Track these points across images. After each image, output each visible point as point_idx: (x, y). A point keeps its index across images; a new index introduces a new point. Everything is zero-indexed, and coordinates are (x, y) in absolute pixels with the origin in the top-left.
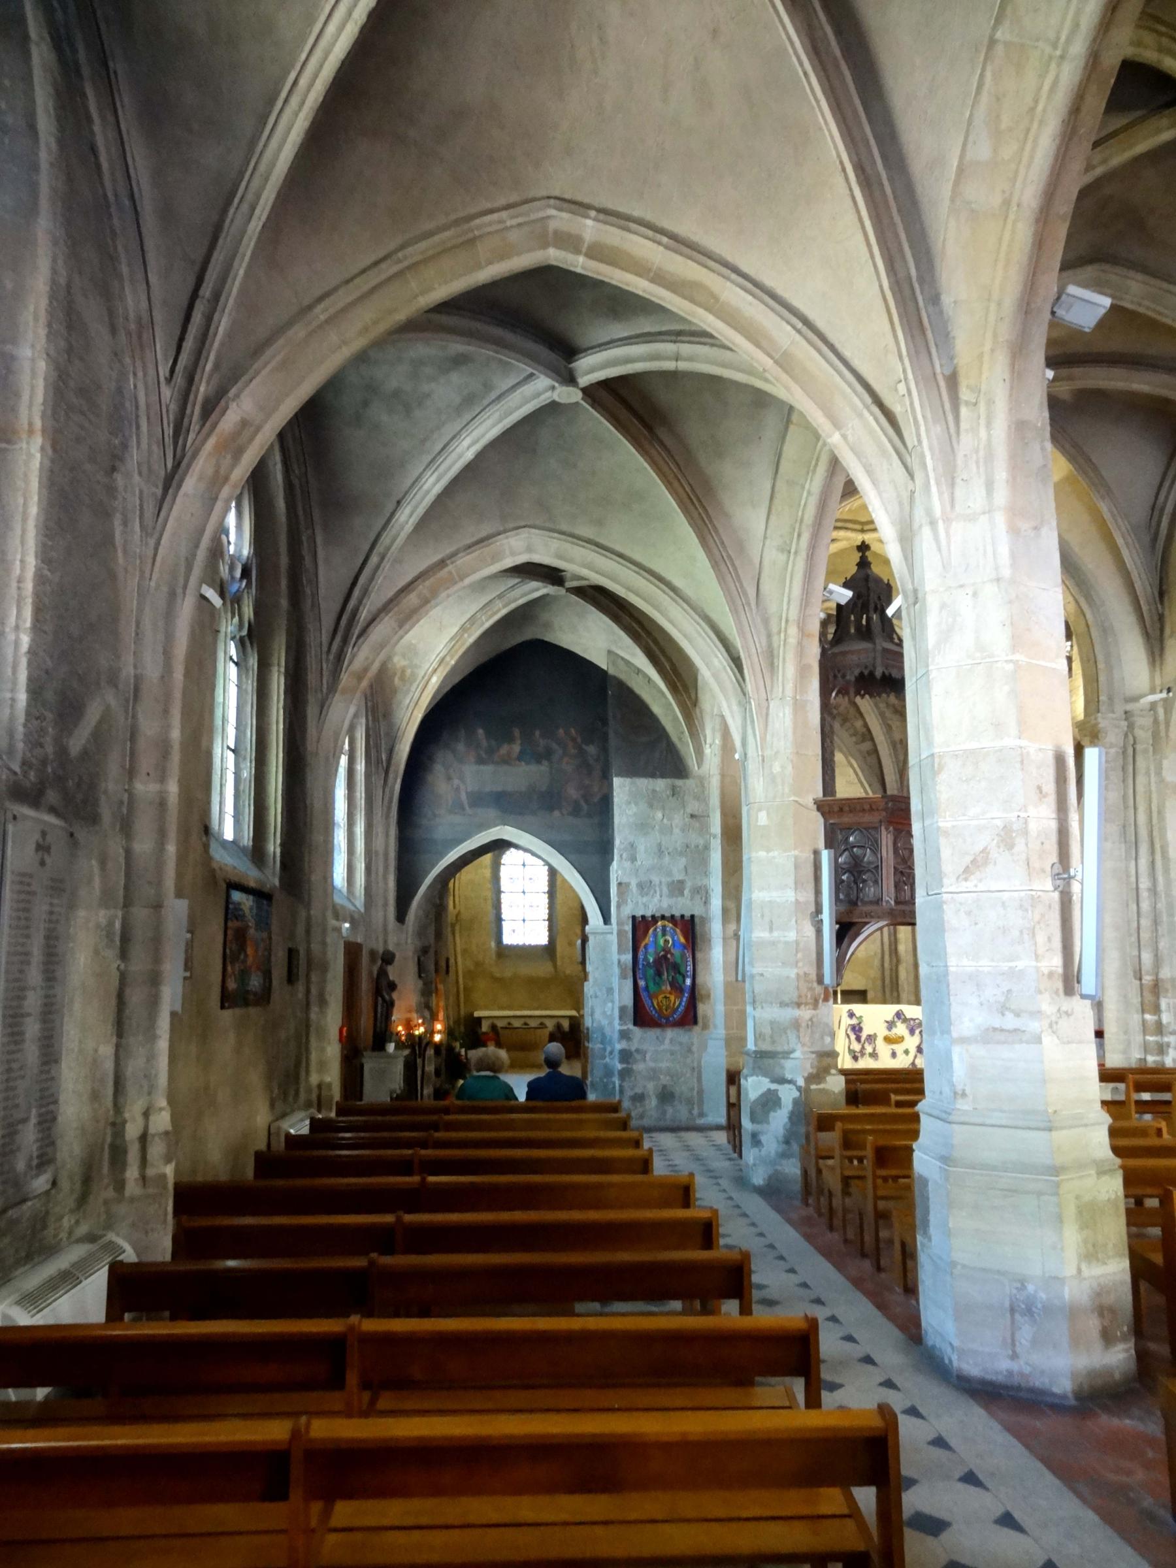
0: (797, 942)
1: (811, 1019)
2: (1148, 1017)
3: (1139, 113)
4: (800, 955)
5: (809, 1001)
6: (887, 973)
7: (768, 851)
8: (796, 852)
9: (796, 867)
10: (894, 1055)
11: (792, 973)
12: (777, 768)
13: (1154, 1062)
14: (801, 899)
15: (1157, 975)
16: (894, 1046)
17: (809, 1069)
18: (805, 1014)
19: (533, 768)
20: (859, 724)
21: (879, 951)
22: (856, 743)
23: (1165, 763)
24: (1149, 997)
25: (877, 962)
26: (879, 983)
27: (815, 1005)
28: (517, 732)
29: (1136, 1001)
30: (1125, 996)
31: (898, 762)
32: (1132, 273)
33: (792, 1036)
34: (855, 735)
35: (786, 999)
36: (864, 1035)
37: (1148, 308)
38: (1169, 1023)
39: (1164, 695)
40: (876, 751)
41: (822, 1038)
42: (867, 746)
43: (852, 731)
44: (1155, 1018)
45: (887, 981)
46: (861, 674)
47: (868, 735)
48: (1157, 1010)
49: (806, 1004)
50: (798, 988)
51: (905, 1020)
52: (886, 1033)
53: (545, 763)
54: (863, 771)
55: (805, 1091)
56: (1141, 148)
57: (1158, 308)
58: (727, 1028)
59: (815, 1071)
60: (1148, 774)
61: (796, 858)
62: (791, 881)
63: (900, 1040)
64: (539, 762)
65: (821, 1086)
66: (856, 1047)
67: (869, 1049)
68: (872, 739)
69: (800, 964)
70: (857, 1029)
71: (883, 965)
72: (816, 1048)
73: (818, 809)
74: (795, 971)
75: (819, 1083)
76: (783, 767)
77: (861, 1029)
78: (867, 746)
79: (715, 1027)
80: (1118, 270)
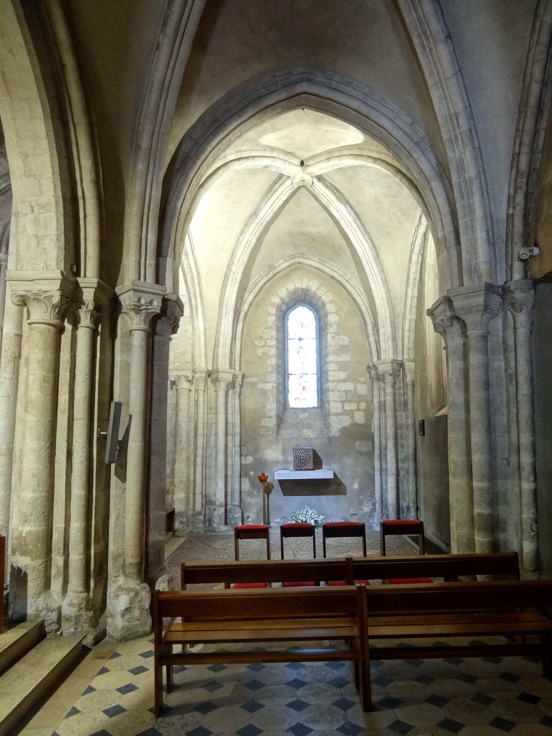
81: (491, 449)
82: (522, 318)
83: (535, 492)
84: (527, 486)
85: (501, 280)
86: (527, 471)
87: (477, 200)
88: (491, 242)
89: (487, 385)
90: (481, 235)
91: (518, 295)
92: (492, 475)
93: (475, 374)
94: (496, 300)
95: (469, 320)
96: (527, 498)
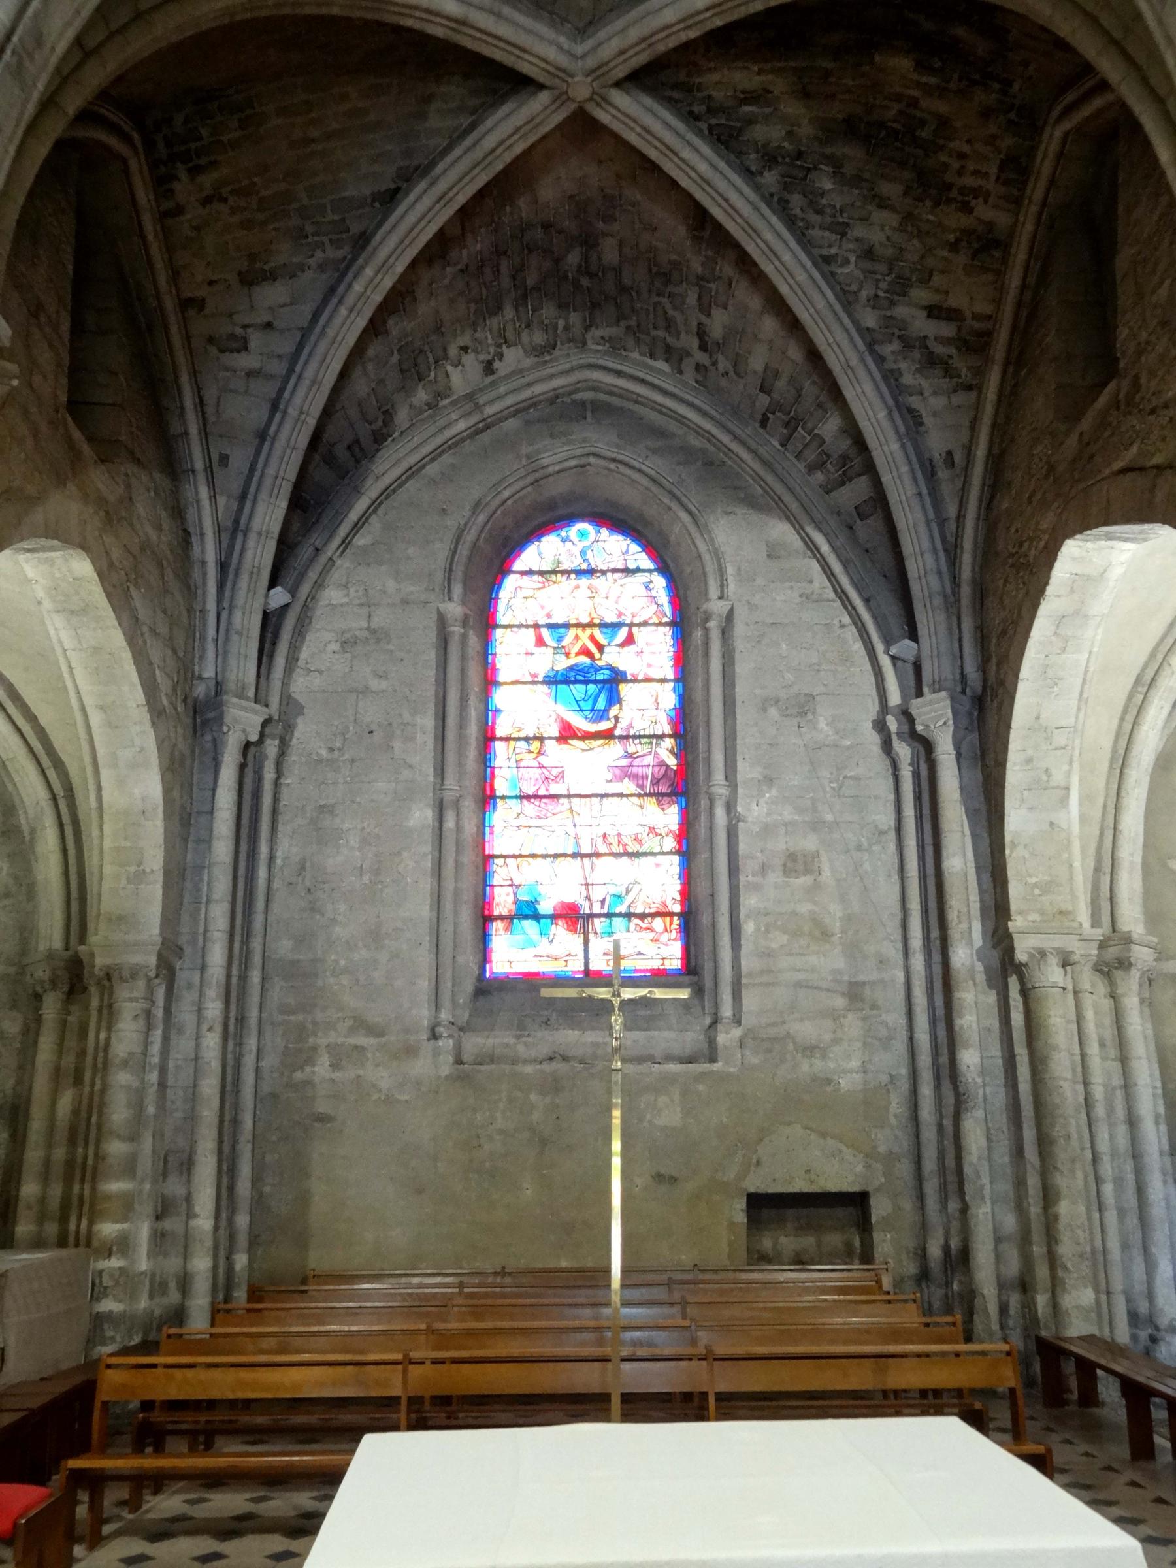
6: (929, 1135)
20: (830, 427)
21: (904, 1071)
25: (896, 1105)
26: (904, 1168)
31: (942, 522)
34: (817, 466)
42: (857, 491)
43: (811, 456)
45: (930, 1164)
54: (845, 564)
68: (870, 468)
78: (857, 491)
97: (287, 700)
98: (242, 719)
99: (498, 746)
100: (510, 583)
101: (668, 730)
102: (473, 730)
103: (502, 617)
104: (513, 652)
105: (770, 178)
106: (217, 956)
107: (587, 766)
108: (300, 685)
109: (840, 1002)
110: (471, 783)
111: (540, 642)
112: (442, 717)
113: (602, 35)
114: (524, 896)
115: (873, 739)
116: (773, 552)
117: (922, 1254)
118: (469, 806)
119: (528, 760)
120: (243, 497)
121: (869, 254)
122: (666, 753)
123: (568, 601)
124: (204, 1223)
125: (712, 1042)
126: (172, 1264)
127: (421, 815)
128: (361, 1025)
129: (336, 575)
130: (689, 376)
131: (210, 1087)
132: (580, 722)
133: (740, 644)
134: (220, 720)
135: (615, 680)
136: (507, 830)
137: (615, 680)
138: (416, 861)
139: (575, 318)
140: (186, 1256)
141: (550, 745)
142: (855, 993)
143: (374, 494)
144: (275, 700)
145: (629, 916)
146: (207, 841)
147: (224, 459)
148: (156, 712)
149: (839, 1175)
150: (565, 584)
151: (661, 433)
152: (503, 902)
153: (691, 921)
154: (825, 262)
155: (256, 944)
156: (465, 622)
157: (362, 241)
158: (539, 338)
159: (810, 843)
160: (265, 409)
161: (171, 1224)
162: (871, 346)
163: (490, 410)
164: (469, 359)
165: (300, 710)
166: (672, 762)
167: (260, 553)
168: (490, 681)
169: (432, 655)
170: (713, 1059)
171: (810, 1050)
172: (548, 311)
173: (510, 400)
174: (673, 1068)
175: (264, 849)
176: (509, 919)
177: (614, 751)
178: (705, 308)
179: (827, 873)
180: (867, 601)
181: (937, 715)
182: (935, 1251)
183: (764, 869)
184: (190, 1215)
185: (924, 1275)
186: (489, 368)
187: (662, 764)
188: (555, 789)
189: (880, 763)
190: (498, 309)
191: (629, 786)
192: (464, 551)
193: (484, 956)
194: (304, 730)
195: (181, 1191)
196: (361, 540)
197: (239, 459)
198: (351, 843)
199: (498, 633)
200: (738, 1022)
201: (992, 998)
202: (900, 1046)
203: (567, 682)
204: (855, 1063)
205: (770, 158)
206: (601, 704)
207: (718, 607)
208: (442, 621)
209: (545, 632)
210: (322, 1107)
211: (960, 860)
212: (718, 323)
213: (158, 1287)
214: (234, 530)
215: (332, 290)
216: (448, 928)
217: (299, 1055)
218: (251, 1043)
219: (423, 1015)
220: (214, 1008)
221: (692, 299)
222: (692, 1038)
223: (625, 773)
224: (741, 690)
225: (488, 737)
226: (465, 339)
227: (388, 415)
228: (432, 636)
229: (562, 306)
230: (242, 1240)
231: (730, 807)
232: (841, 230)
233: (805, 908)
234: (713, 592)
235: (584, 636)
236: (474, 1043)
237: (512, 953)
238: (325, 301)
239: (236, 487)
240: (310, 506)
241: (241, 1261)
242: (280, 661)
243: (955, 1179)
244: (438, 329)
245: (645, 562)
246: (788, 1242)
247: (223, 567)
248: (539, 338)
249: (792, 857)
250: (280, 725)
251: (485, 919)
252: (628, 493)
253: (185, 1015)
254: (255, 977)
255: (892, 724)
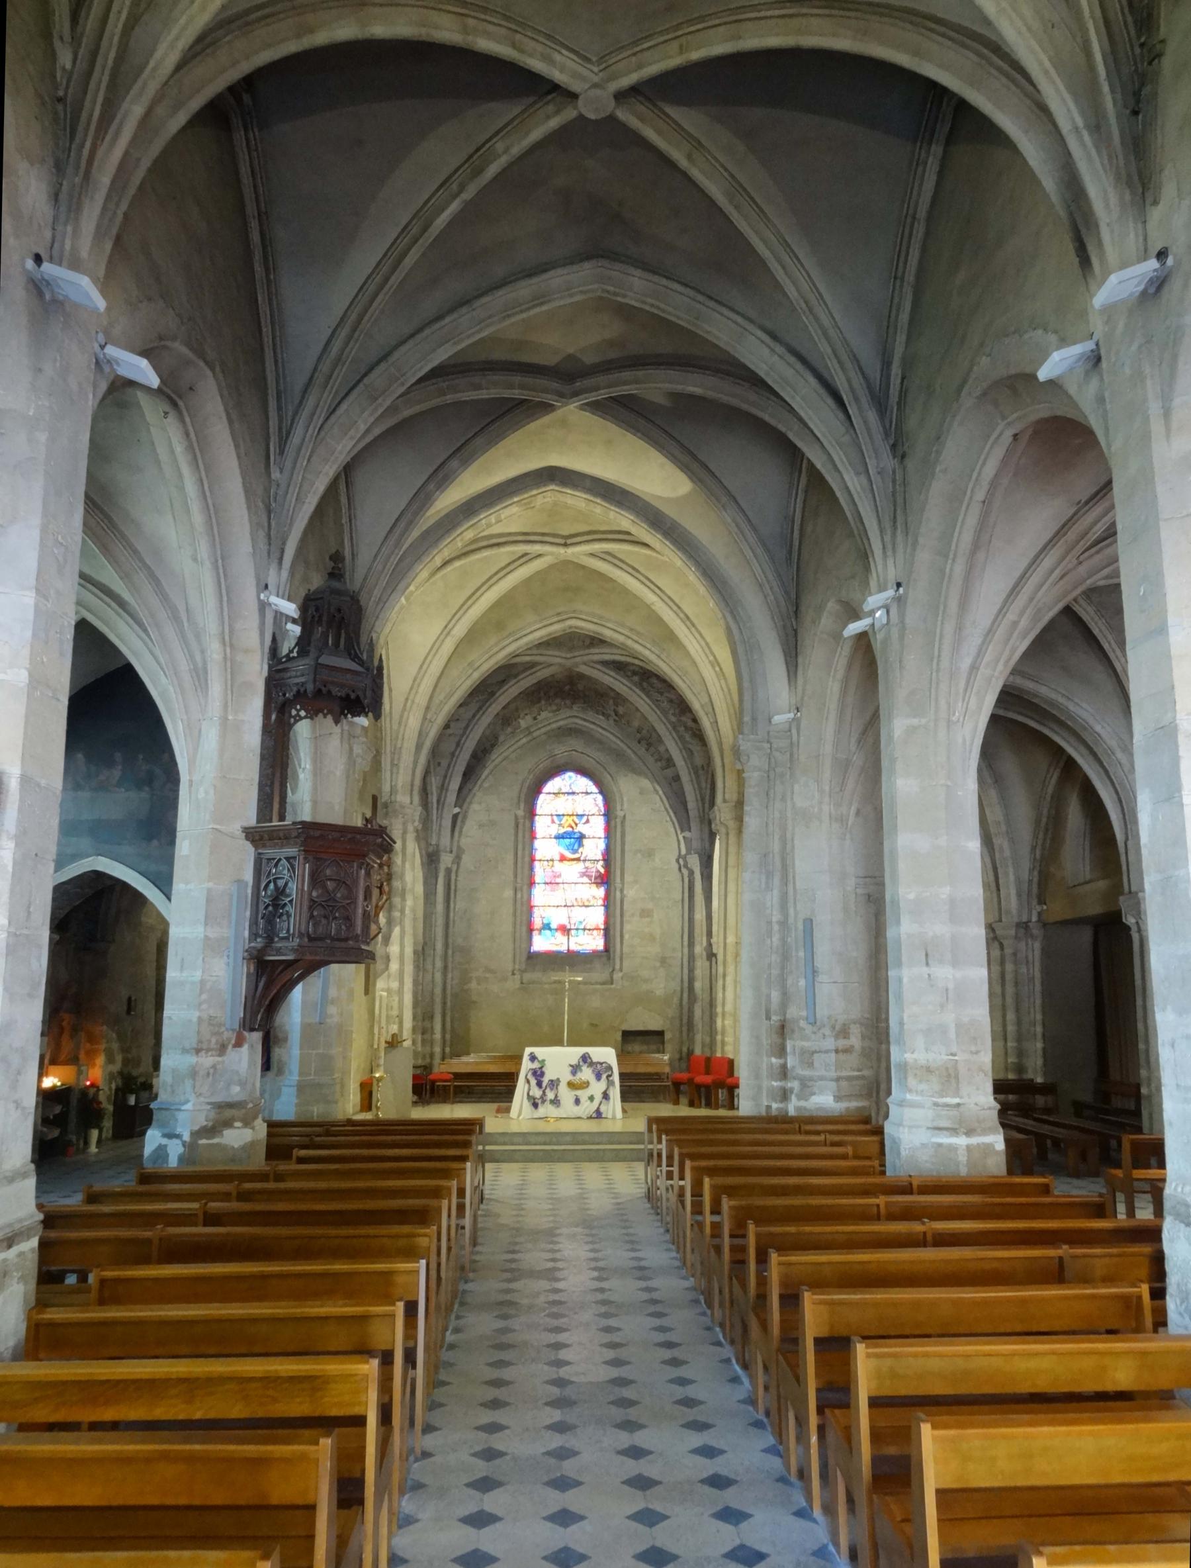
0: (203, 982)
1: (214, 1067)
2: (774, 1060)
3: (531, 99)
4: (204, 997)
5: (213, 1045)
6: (685, 1010)
7: (187, 883)
8: (211, 885)
9: (209, 900)
10: (577, 1101)
11: (194, 1015)
12: (201, 795)
13: (777, 1109)
14: (211, 935)
15: (785, 1015)
16: (579, 1093)
17: (201, 1121)
18: (207, 1061)
19: (133, 794)
22: (663, 769)
23: (796, 787)
24: (776, 1039)
25: (676, 1000)
26: (677, 1022)
27: (222, 1050)
28: (118, 756)
29: (765, 1042)
30: (757, 1038)
31: (700, 788)
32: (632, 270)
33: (188, 1083)
35: (187, 1046)
36: (545, 1080)
37: (652, 305)
38: (794, 1067)
39: (791, 715)
40: (677, 778)
41: (228, 1086)
42: (669, 772)
44: (781, 1061)
46: (298, 691)
47: (670, 762)
48: (781, 1051)
49: (208, 1050)
50: (198, 1032)
51: (591, 1064)
52: (570, 1077)
53: (147, 789)
55: (191, 1147)
56: (536, 135)
57: (662, 306)
58: (300, 1074)
59: (210, 1124)
60: (783, 799)
61: (209, 890)
62: (201, 916)
63: (586, 1085)
64: (139, 787)
65: (215, 1141)
66: (537, 1093)
67: (550, 1095)
69: (204, 1006)
70: (538, 1074)
71: (681, 1005)
72: (219, 1098)
73: (247, 838)
74: (197, 1014)
75: (213, 1138)
76: (206, 793)
77: (542, 1074)
79: (291, 1073)
80: (618, 266)
81: (1019, 1023)
82: (1037, 945)
83: (1044, 1050)
84: (1039, 1045)
85: (1025, 919)
86: (1039, 1036)
87: (1011, 870)
88: (1019, 895)
89: (1016, 984)
90: (1013, 892)
91: (1035, 932)
92: (1019, 1038)
93: (1009, 977)
94: (1022, 931)
95: (1005, 943)
96: (1040, 1052)
97: (459, 847)
98: (446, 860)
99: (537, 864)
100: (542, 797)
101: (600, 857)
102: (527, 859)
103: (538, 811)
104: (543, 826)
105: (636, 678)
106: (439, 946)
107: (570, 872)
108: (464, 841)
109: (658, 964)
110: (526, 881)
111: (553, 822)
112: (516, 854)
113: (576, 654)
114: (546, 921)
115: (677, 866)
116: (642, 792)
117: (681, 1052)
118: (525, 887)
119: (548, 869)
120: (445, 777)
121: (671, 701)
122: (600, 867)
123: (563, 805)
124: (438, 1036)
125: (612, 978)
126: (428, 1049)
127: (508, 893)
128: (488, 970)
129: (476, 799)
130: (611, 722)
131: (438, 991)
132: (569, 855)
133: (628, 829)
134: (438, 861)
135: (582, 837)
136: (540, 895)
137: (582, 837)
138: (507, 910)
139: (568, 702)
140: (432, 1046)
141: (556, 863)
142: (663, 961)
143: (491, 767)
144: (455, 849)
145: (584, 929)
146: (434, 904)
147: (439, 764)
148: (422, 864)
149: (654, 1024)
150: (563, 798)
151: (600, 742)
152: (537, 922)
153: (607, 932)
154: (656, 702)
155: (450, 941)
156: (525, 817)
157: (493, 694)
158: (554, 708)
159: (650, 906)
160: (454, 745)
161: (427, 1036)
162: (674, 728)
163: (535, 734)
164: (529, 718)
165: (464, 851)
166: (602, 871)
167: (452, 797)
168: (533, 836)
169: (513, 831)
170: (612, 983)
171: (646, 981)
172: (558, 701)
173: (543, 730)
174: (598, 986)
175: (452, 905)
176: (540, 930)
177: (580, 867)
178: (616, 704)
179: (655, 916)
180: (675, 813)
181: (695, 862)
182: (685, 1049)
183: (633, 915)
184: (433, 1033)
185: (681, 1059)
186: (535, 719)
187: (598, 871)
188: (558, 880)
189: (678, 876)
190: (539, 701)
191: (585, 880)
192: (525, 790)
193: (530, 943)
194: (466, 859)
195: (429, 1026)
196: (486, 785)
197: (444, 763)
198: (484, 903)
199: (537, 818)
200: (621, 970)
201: (708, 964)
202: (678, 980)
203: (563, 838)
204: (662, 986)
205: (634, 673)
206: (576, 847)
207: (620, 814)
208: (516, 817)
209: (555, 818)
210: (474, 998)
211: (700, 915)
212: (621, 710)
213: (424, 1057)
214: (443, 788)
215: (480, 708)
216: (518, 935)
217: (465, 979)
218: (450, 976)
219: (510, 969)
220: (439, 964)
221: (611, 702)
222: (605, 976)
223: (584, 874)
224: (627, 848)
225: (533, 860)
226: (527, 711)
227: (497, 738)
228: (513, 824)
229: (563, 699)
230: (448, 1043)
231: (622, 891)
232: (662, 694)
233: (646, 930)
234: (618, 808)
235: (570, 820)
236: (527, 976)
237: (541, 943)
238: (478, 711)
239: (443, 773)
240: (470, 774)
241: (448, 1050)
242: (456, 834)
243: (690, 1025)
244: (517, 709)
245: (594, 789)
246: (637, 1047)
247: (438, 801)
248: (554, 708)
249: (643, 910)
250: (458, 859)
251: (531, 930)
252: (588, 762)
253: (429, 967)
254: (450, 952)
255: (681, 861)
